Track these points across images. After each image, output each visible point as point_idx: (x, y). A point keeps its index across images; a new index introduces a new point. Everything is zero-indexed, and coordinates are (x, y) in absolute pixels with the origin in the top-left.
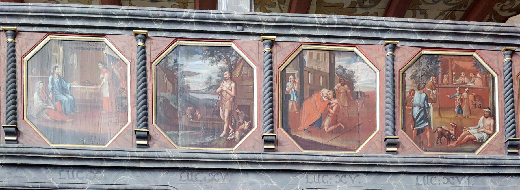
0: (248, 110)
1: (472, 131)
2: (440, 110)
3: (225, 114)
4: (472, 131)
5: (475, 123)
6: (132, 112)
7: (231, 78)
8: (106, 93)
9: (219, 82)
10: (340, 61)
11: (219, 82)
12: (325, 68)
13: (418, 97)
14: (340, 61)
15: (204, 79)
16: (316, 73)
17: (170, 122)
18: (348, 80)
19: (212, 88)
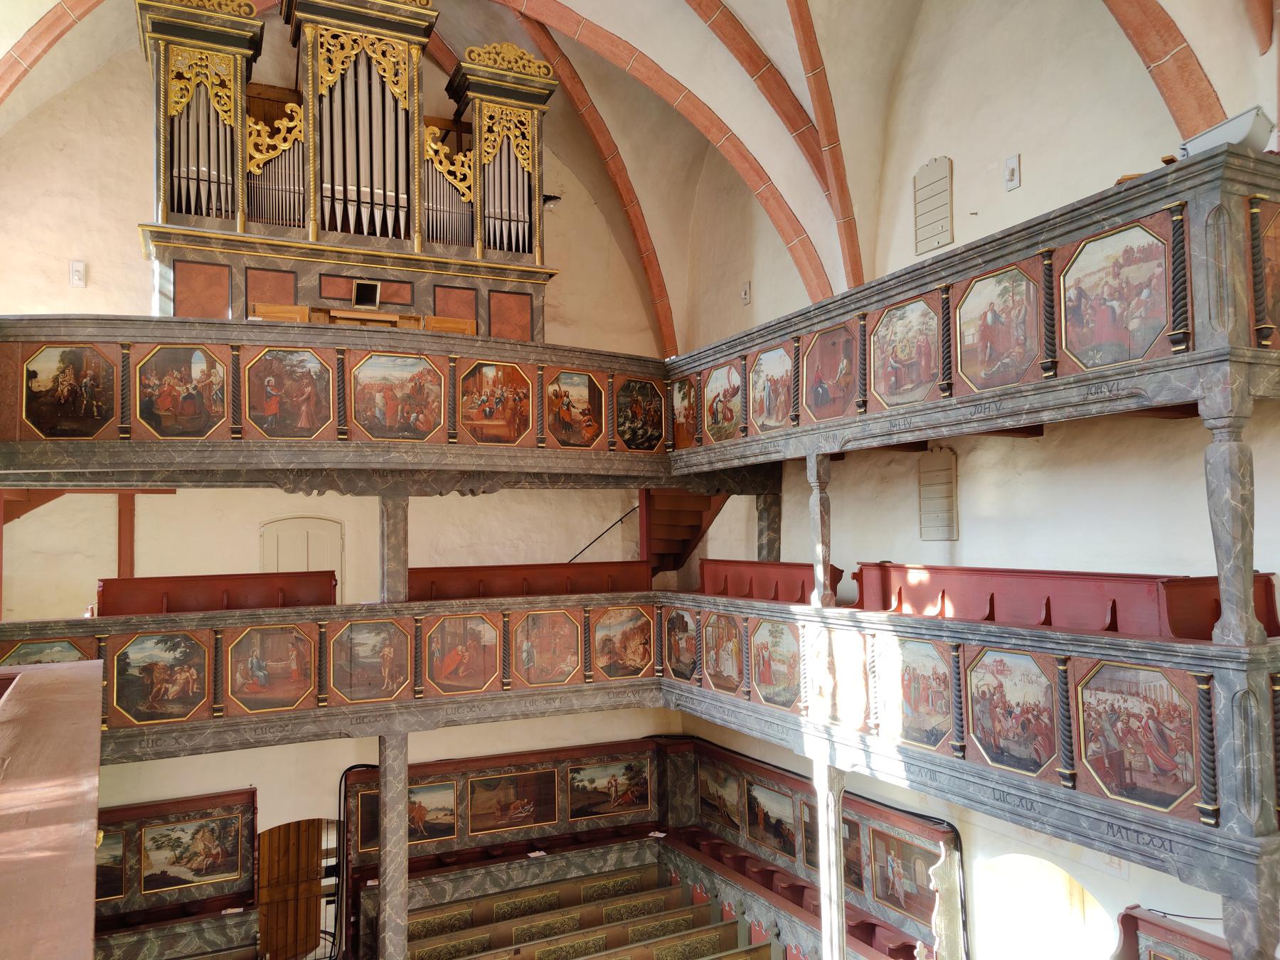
0: (401, 669)
1: (563, 666)
2: (540, 653)
3: (386, 672)
4: (563, 666)
5: (564, 660)
6: (314, 678)
7: (390, 645)
8: (294, 666)
9: (382, 649)
10: (471, 625)
11: (382, 649)
12: (461, 631)
13: (525, 646)
14: (471, 625)
15: (370, 647)
16: (455, 635)
17: (346, 681)
18: (476, 636)
19: (376, 651)
